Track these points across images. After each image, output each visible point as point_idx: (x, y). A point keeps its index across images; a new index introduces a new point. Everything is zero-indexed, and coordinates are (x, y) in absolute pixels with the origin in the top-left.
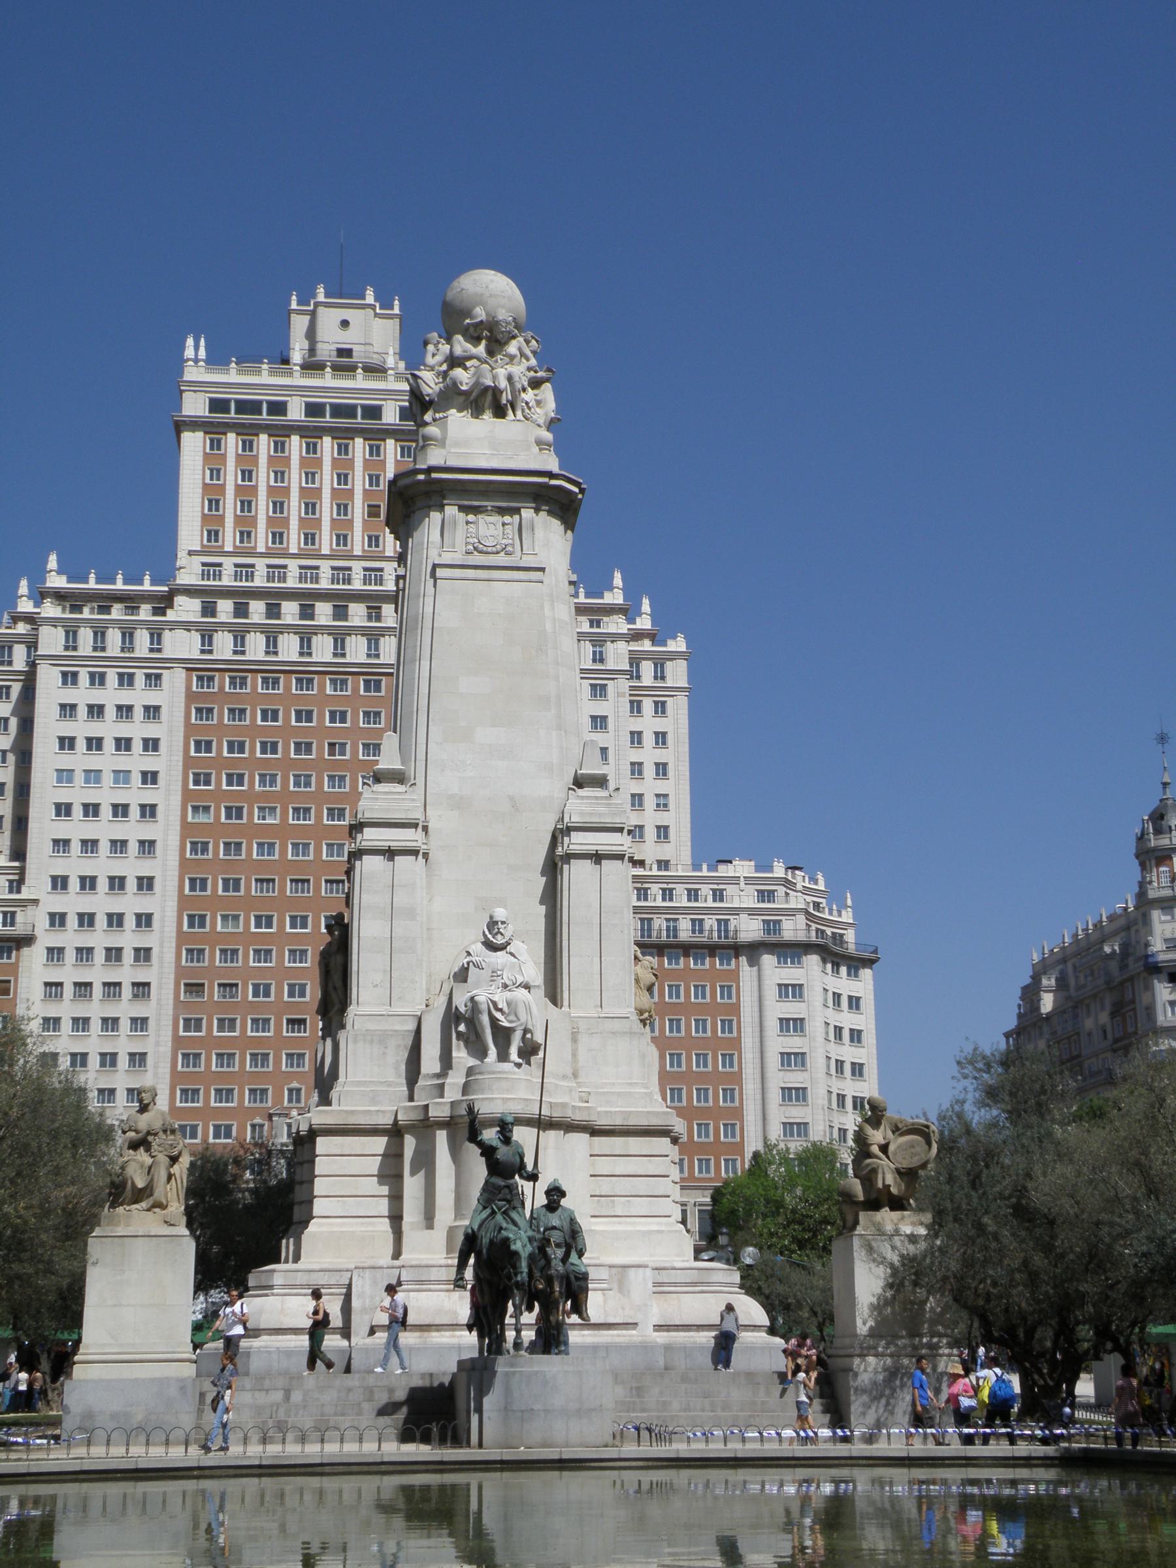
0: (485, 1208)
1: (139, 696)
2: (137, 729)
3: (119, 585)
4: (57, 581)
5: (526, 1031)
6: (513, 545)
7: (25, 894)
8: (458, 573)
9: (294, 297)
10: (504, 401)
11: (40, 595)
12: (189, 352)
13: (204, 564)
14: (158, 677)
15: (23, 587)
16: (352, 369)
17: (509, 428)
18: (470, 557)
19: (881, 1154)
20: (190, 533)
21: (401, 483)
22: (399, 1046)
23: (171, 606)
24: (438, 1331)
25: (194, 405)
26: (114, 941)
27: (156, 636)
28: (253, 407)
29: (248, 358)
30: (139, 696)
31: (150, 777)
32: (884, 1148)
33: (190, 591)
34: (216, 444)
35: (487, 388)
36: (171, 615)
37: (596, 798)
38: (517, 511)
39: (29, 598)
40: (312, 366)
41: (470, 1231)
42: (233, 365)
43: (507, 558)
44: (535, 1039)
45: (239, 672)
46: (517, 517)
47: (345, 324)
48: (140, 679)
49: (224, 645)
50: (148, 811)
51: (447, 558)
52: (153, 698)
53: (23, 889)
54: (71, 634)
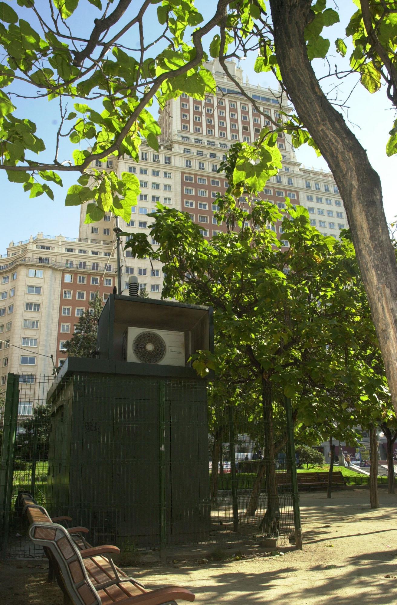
1: (161, 180)
30: (161, 180)
48: (161, 174)
49: (195, 165)
52: (168, 182)
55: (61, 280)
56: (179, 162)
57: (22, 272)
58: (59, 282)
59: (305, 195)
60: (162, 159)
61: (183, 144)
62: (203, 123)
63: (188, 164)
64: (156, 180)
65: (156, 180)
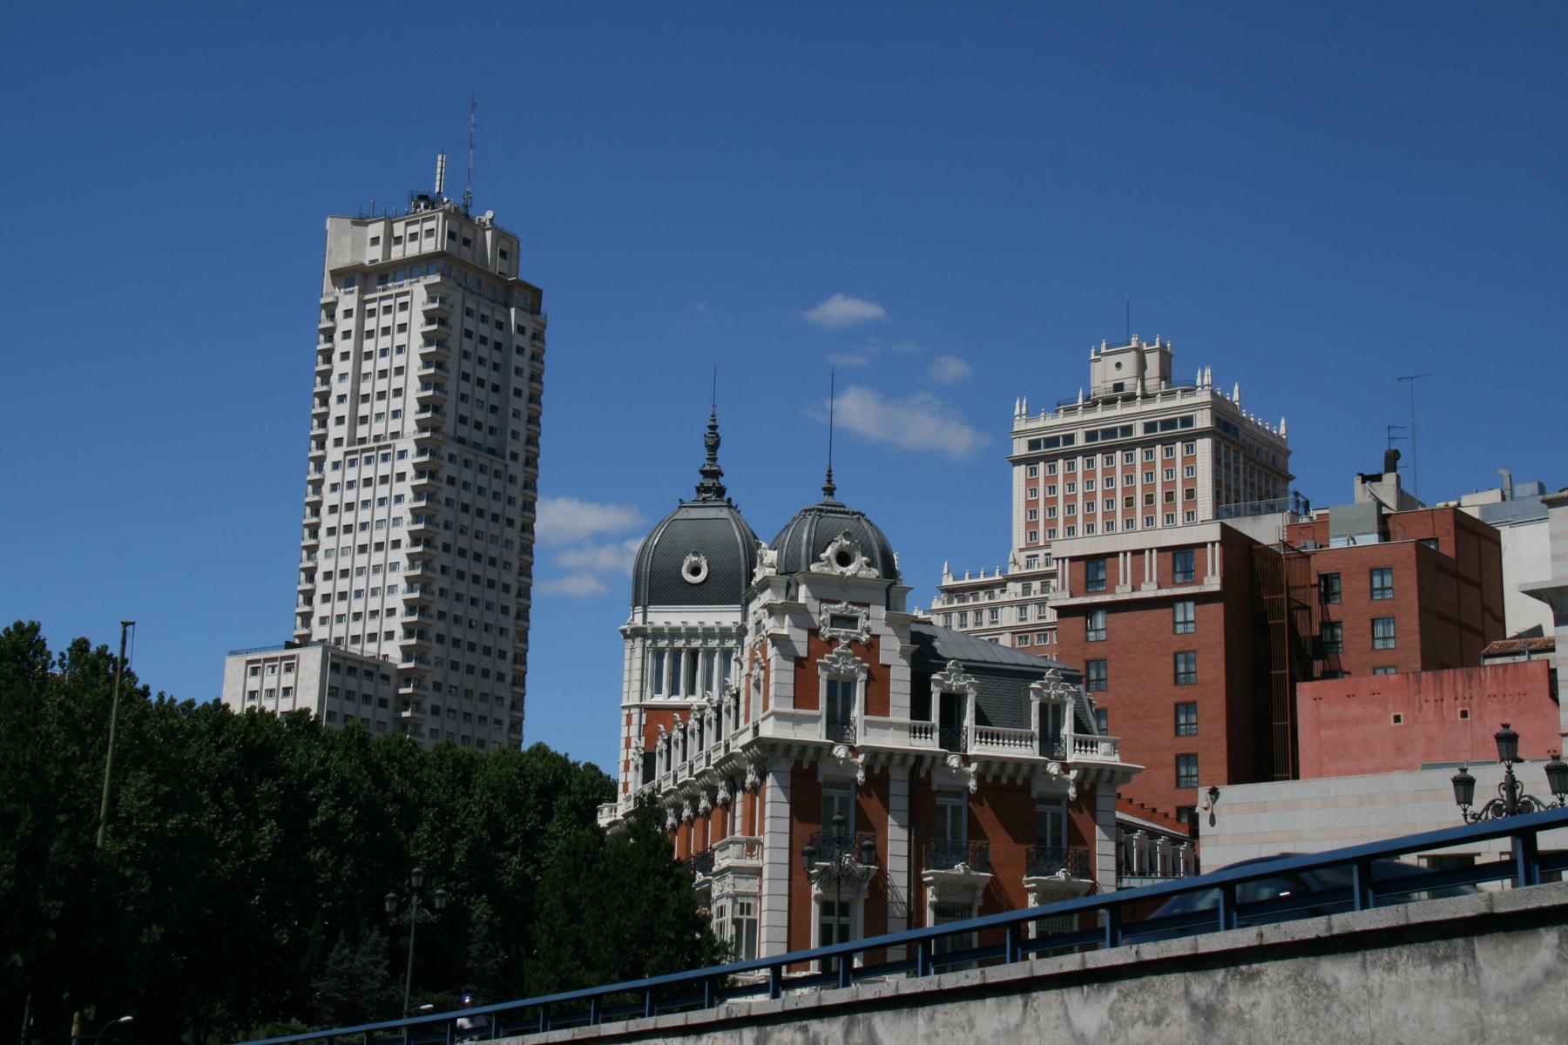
3: (982, 579)
4: (948, 581)
12: (1017, 412)
13: (1028, 557)
20: (1019, 537)
25: (1020, 448)
27: (994, 610)
28: (1052, 442)
33: (1016, 579)
34: (1033, 471)
40: (1091, 404)
47: (1118, 365)
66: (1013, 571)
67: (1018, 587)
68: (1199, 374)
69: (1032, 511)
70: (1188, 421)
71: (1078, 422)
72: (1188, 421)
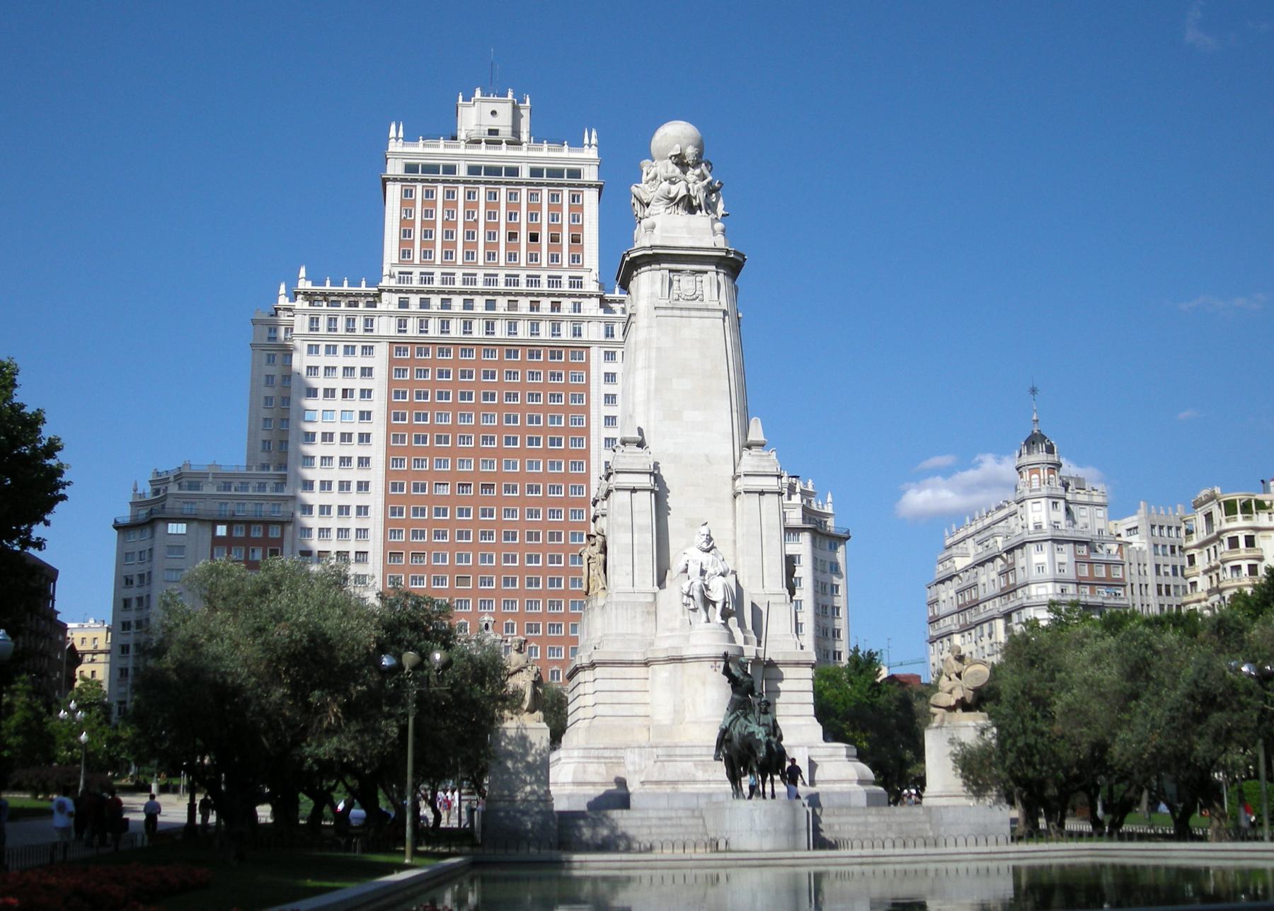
0: (732, 714)
1: (358, 361)
2: (357, 383)
4: (304, 285)
5: (725, 604)
6: (703, 295)
7: (287, 492)
8: (669, 312)
9: (461, 98)
10: (695, 203)
11: (294, 296)
12: (393, 133)
14: (371, 347)
15: (282, 289)
16: (500, 143)
17: (701, 219)
18: (677, 302)
19: (957, 679)
21: (631, 256)
22: (643, 612)
23: (381, 302)
24: (683, 784)
26: (343, 524)
27: (369, 322)
28: (433, 169)
29: (432, 136)
30: (358, 361)
31: (365, 416)
32: (959, 675)
35: (684, 196)
36: (380, 307)
37: (761, 456)
38: (706, 272)
39: (286, 295)
41: (724, 727)
42: (421, 141)
43: (701, 303)
44: (731, 608)
45: (422, 347)
46: (705, 277)
47: (494, 113)
48: (358, 350)
49: (412, 328)
50: (365, 438)
51: (664, 303)
52: (367, 362)
53: (285, 489)
54: (314, 321)
55: (210, 533)
56: (386, 327)
57: (160, 526)
58: (208, 537)
59: (603, 350)
60: (359, 324)
61: (398, 291)
62: (437, 241)
63: (402, 324)
64: (349, 361)
65: (349, 361)
66: (386, 282)
67: (395, 298)
68: (586, 134)
69: (406, 233)
70: (575, 174)
71: (458, 154)
72: (575, 174)
